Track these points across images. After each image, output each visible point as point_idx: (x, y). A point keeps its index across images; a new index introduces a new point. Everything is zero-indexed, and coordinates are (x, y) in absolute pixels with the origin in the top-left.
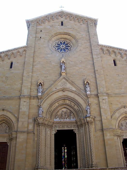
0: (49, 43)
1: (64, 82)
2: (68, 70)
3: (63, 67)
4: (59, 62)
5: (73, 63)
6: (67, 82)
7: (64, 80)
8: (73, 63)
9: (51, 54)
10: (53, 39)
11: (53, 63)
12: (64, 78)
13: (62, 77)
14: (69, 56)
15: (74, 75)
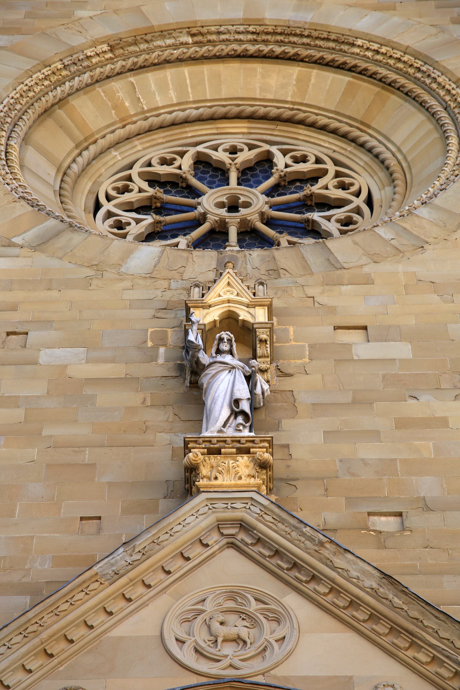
0: (26, 140)
1: (233, 595)
2: (305, 439)
3: (225, 385)
4: (161, 340)
5: (401, 350)
6: (292, 601)
7: (233, 569)
8: (401, 350)
9: (40, 245)
10: (92, 112)
11: (45, 357)
12: (241, 536)
13: (194, 517)
14: (333, 264)
15: (426, 507)
